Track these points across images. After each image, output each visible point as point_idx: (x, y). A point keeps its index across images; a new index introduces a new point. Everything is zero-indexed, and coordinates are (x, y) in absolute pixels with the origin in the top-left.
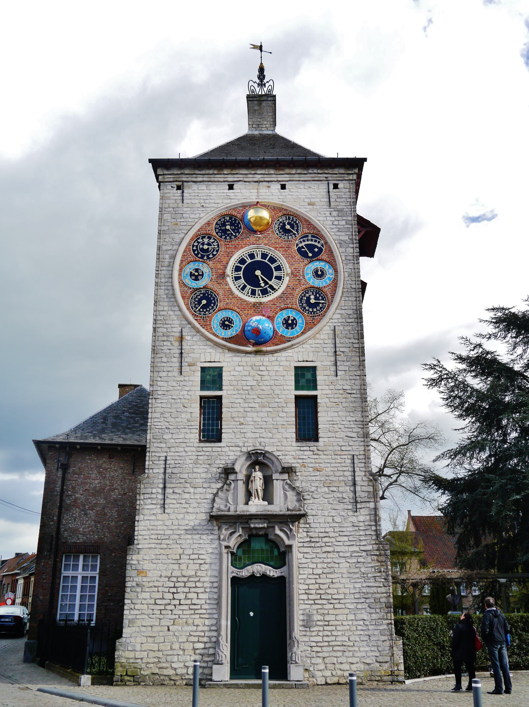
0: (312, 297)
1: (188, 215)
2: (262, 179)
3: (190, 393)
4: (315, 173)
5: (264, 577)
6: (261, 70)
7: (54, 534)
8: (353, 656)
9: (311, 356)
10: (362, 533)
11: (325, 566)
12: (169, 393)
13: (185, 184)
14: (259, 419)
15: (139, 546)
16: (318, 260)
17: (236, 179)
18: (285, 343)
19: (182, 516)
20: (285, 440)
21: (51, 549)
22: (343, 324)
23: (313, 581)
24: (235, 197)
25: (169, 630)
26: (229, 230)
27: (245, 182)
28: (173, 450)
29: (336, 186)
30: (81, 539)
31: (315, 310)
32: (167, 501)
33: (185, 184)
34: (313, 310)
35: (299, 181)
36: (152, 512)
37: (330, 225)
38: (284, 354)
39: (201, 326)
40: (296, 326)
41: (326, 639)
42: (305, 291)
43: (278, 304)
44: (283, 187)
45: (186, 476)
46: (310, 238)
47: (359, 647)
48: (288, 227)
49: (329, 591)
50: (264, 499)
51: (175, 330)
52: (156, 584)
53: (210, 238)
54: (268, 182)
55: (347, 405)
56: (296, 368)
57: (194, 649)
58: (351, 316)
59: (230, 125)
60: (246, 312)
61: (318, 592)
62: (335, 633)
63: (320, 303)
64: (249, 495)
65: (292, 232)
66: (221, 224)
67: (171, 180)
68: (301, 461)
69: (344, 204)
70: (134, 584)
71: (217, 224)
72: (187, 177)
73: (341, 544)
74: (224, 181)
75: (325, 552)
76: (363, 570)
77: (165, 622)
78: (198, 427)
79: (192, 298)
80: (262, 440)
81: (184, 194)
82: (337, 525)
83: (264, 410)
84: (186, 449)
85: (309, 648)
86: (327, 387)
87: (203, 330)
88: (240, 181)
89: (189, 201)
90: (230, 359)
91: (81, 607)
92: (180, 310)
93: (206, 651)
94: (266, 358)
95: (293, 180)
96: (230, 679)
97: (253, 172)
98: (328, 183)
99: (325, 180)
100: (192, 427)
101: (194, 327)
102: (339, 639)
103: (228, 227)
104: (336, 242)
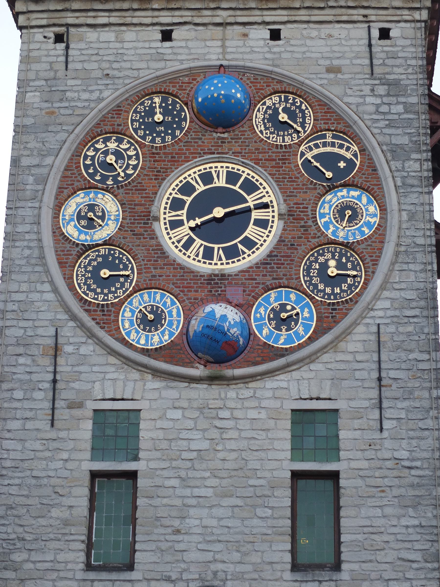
0: (332, 263)
1: (76, 94)
3: (70, 465)
4: (341, 7)
9: (328, 387)
12: (26, 465)
13: (72, 30)
14: (214, 523)
16: (345, 185)
18: (272, 359)
20: (268, 567)
22: (395, 320)
24: (174, 57)
29: (385, 34)
31: (337, 290)
34: (333, 290)
35: (308, 22)
37: (371, 114)
38: (270, 383)
39: (98, 323)
40: (296, 324)
42: (318, 252)
43: (259, 279)
44: (275, 35)
48: (283, 117)
51: (40, 331)
53: (120, 141)
55: (402, 491)
58: (414, 304)
60: (192, 294)
63: (349, 276)
65: (292, 127)
66: (145, 111)
67: (44, 22)
69: (401, 70)
71: (135, 111)
72: (77, 17)
78: (84, 538)
80: (220, 566)
81: (71, 52)
83: (226, 502)
86: (359, 454)
87: (101, 333)
88: (185, 23)
89: (79, 66)
90: (156, 395)
92: (55, 290)
95: (295, 22)
98: (369, 27)
99: (362, 22)
100: (72, 537)
101: (82, 326)
104: (384, 148)
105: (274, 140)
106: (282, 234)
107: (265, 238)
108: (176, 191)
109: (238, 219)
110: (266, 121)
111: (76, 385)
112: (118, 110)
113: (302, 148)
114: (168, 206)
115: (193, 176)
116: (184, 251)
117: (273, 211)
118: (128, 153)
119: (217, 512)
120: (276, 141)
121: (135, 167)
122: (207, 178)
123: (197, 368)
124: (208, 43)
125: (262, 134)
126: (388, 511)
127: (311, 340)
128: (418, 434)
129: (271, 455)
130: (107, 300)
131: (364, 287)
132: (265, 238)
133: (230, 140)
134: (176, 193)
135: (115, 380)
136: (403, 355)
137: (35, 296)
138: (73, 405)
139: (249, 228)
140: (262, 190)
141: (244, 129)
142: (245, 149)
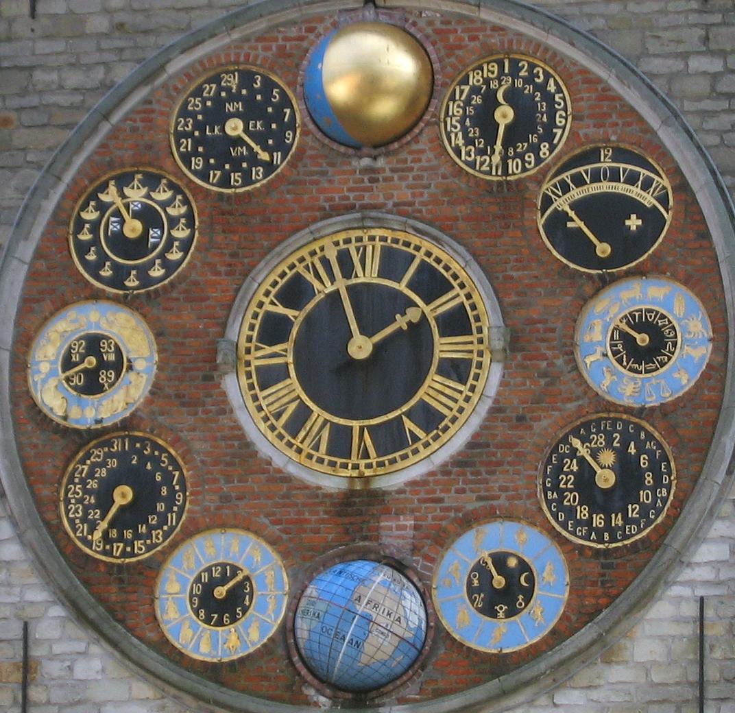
0: (608, 458)
1: (54, 76)
16: (639, 272)
26: (238, 141)
34: (608, 521)
37: (699, 99)
40: (528, 600)
43: (450, 499)
46: (606, 164)
53: (152, 182)
66: (205, 111)
71: (184, 113)
79: (71, 481)
103: (235, 127)
105: (485, 168)
106: (499, 394)
107: (461, 403)
108: (271, 297)
109: (407, 357)
110: (468, 123)
112: (145, 111)
113: (547, 187)
114: (255, 334)
115: (309, 260)
116: (288, 437)
117: (481, 341)
118: (171, 211)
120: (490, 173)
121: (186, 246)
125: (459, 156)
130: (133, 555)
132: (461, 403)
133: (388, 174)
134: (272, 303)
139: (428, 382)
140: (457, 290)
141: (421, 146)
142: (422, 195)
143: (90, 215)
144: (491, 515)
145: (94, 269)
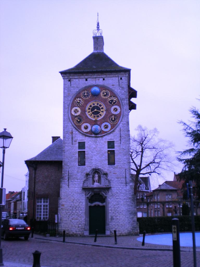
0: (113, 118)
2: (97, 77)
3: (75, 150)
5: (99, 206)
6: (98, 24)
7: (33, 191)
8: (125, 228)
10: (128, 192)
11: (116, 202)
13: (71, 79)
14: (96, 158)
15: (62, 198)
16: (115, 105)
17: (88, 77)
19: (74, 188)
21: (32, 196)
23: (113, 207)
25: (71, 221)
27: (91, 78)
28: (70, 168)
30: (42, 193)
32: (70, 184)
33: (71, 79)
36: (65, 187)
41: (117, 223)
44: (104, 79)
45: (75, 176)
47: (126, 225)
49: (117, 210)
50: (98, 183)
51: (69, 130)
52: (67, 208)
53: (80, 98)
54: (99, 78)
56: (108, 142)
57: (79, 227)
59: (88, 50)
61: (115, 210)
62: (119, 222)
64: (94, 181)
67: (67, 78)
68: (109, 171)
70: (60, 208)
73: (121, 196)
74: (84, 78)
75: (117, 198)
76: (128, 203)
77: (70, 219)
82: (120, 190)
84: (75, 168)
85: (112, 226)
86: (117, 148)
87: (79, 130)
89: (73, 86)
90: (87, 139)
91: (44, 215)
93: (82, 227)
94: (98, 139)
96: (89, 234)
97: (94, 75)
102: (120, 223)
104: (121, 99)
111: (75, 138)
119: (97, 157)
121: (82, 103)
122: (94, 104)
123: (92, 135)
124: (93, 81)
126: (122, 156)
127: (110, 130)
128: (126, 144)
129: (105, 148)
131: (118, 122)
135: (81, 137)
136: (124, 132)
137: (68, 124)
138: (75, 141)
143: (75, 101)
144: (105, 122)
145: (76, 104)
